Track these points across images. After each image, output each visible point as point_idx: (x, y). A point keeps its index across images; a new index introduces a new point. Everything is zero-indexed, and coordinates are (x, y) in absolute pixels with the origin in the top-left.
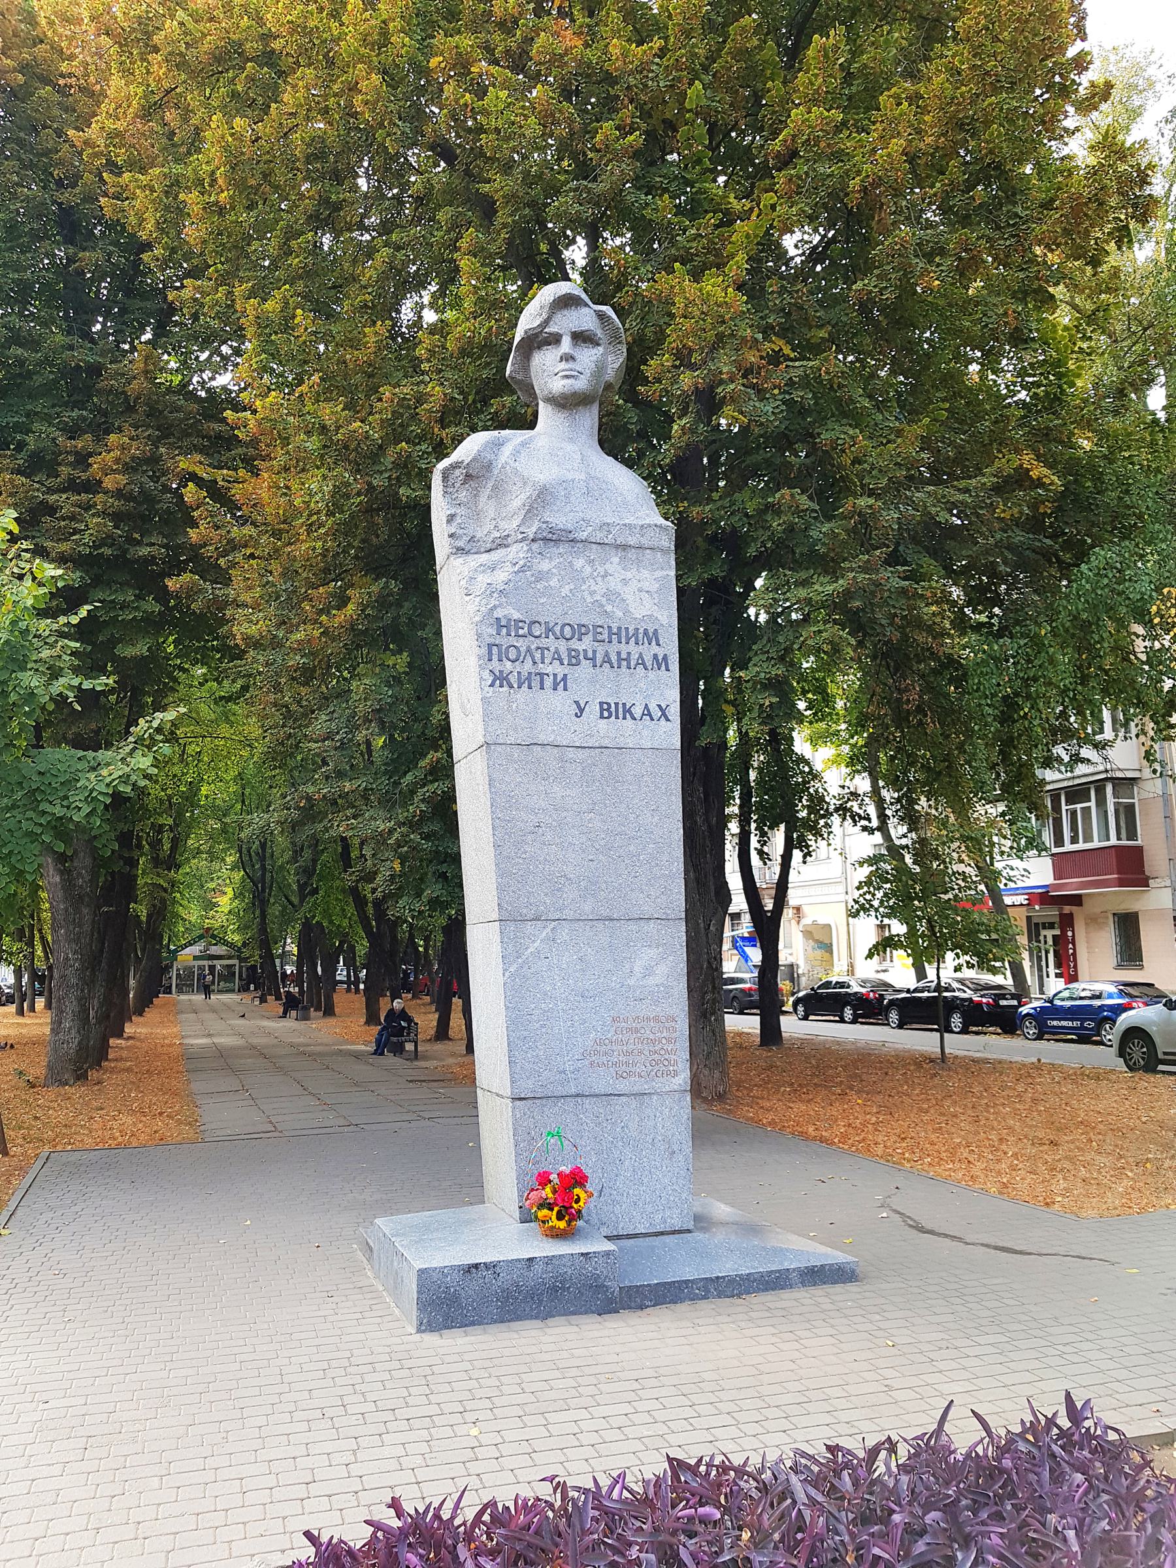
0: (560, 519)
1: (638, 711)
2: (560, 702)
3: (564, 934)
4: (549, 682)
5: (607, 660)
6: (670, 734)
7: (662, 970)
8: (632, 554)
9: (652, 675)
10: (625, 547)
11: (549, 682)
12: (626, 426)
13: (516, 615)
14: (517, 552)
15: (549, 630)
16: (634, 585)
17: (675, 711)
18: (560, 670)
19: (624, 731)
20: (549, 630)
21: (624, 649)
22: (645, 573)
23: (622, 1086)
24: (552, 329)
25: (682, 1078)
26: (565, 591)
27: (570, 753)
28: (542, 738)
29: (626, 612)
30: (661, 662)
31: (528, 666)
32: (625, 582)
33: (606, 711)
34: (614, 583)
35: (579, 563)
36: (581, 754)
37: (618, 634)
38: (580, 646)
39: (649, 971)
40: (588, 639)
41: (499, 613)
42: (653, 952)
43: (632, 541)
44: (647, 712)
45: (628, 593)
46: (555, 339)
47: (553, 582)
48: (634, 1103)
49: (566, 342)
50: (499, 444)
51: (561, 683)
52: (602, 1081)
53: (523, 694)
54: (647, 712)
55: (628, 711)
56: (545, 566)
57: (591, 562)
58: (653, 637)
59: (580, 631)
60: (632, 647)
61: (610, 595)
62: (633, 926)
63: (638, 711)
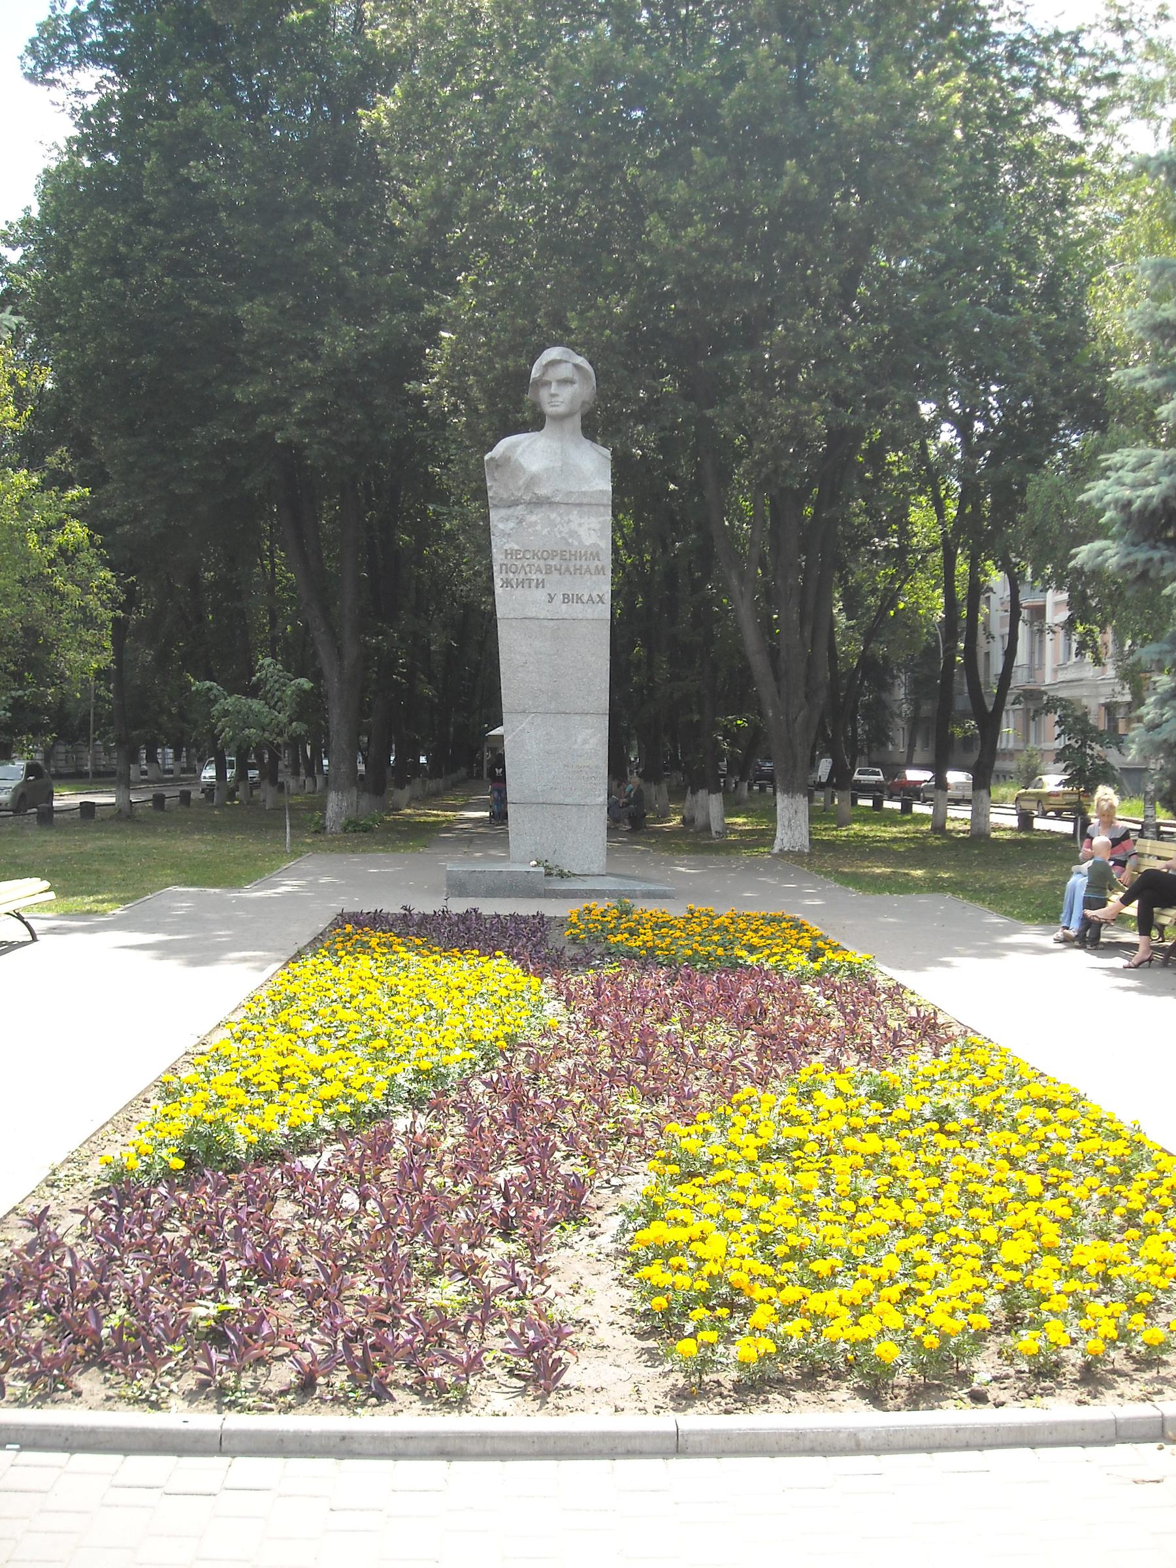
0: (543, 491)
1: (585, 598)
2: (540, 595)
3: (539, 720)
4: (534, 584)
5: (568, 570)
6: (604, 611)
7: (593, 741)
8: (585, 509)
9: (594, 578)
10: (580, 505)
11: (534, 584)
12: (596, 425)
13: (516, 547)
14: (520, 510)
15: (535, 555)
16: (586, 526)
17: (608, 597)
18: (540, 577)
19: (577, 610)
20: (535, 555)
21: (578, 563)
22: (593, 519)
23: (567, 801)
24: (546, 378)
25: (603, 798)
26: (545, 532)
27: (545, 623)
28: (530, 615)
29: (580, 542)
30: (600, 571)
31: (522, 576)
32: (580, 525)
33: (566, 598)
34: (574, 526)
35: (553, 516)
36: (552, 623)
37: (577, 555)
38: (552, 563)
39: (585, 742)
40: (557, 559)
41: (507, 547)
42: (589, 731)
43: (585, 501)
44: (591, 598)
45: (582, 532)
46: (549, 384)
47: (539, 528)
48: (574, 809)
49: (554, 384)
50: (515, 446)
51: (540, 584)
52: (558, 797)
53: (519, 592)
54: (591, 598)
55: (579, 598)
56: (533, 518)
57: (560, 515)
58: (596, 556)
59: (553, 554)
60: (583, 562)
61: (573, 533)
62: (578, 718)
63: (585, 598)
